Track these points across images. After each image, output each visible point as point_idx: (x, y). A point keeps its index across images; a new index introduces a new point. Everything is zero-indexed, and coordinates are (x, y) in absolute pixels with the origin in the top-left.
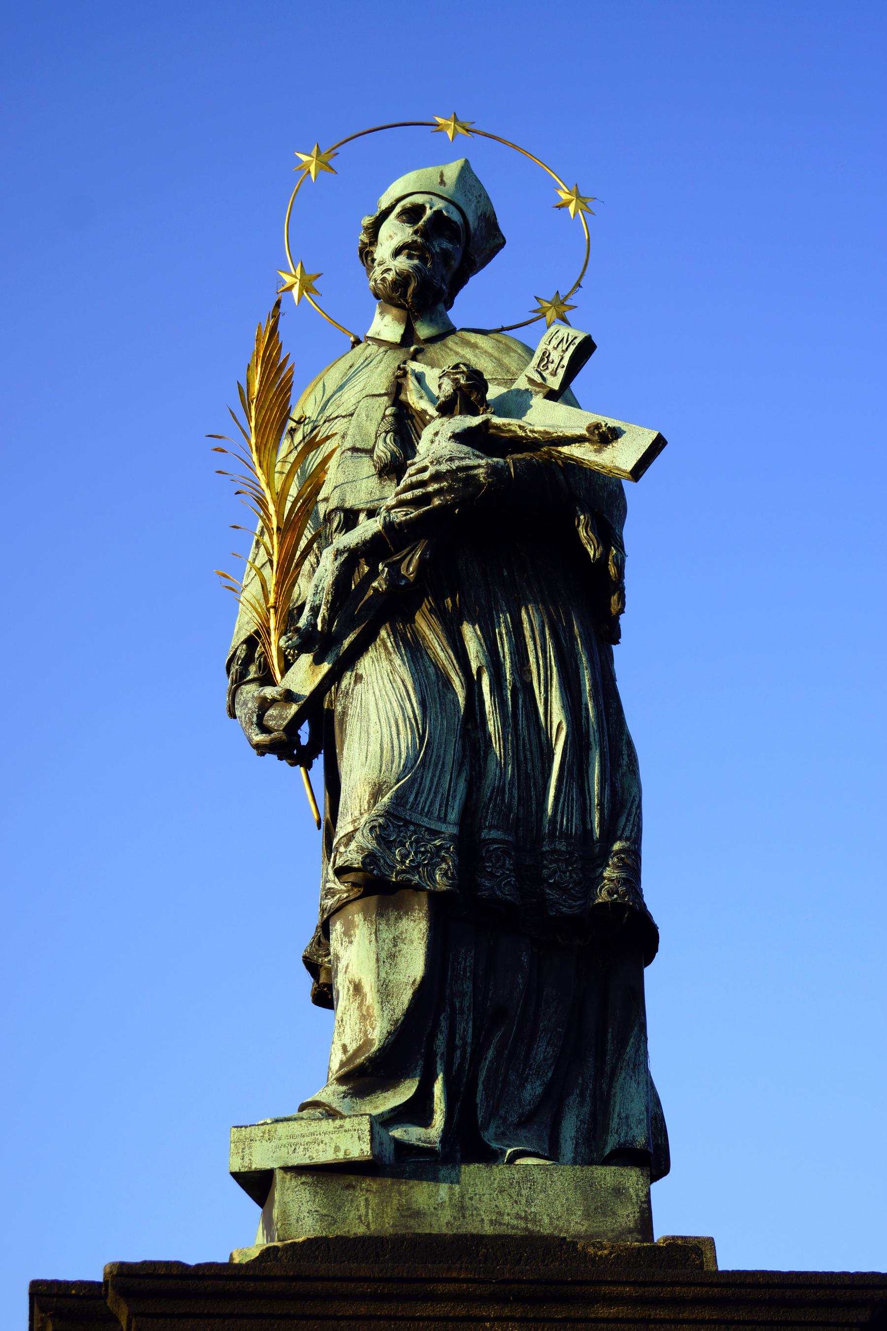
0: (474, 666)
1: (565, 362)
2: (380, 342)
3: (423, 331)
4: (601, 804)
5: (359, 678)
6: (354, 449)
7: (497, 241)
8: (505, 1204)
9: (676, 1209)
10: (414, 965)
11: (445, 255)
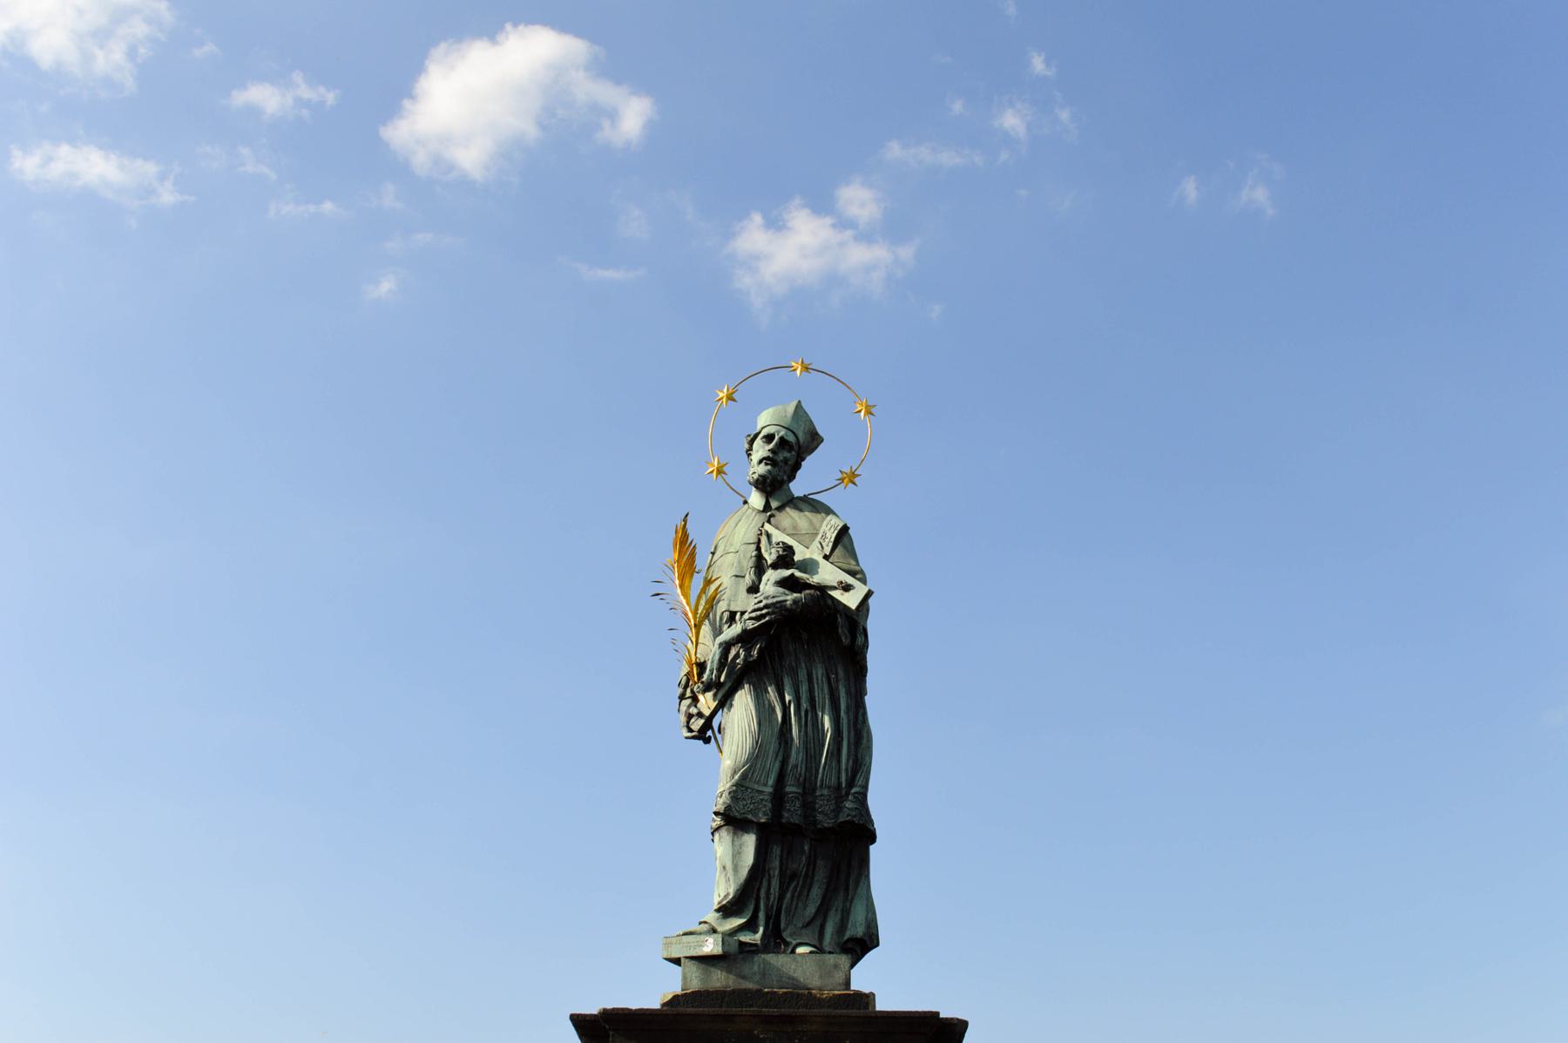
3: (774, 504)
9: (865, 976)
10: (749, 858)
11: (786, 461)
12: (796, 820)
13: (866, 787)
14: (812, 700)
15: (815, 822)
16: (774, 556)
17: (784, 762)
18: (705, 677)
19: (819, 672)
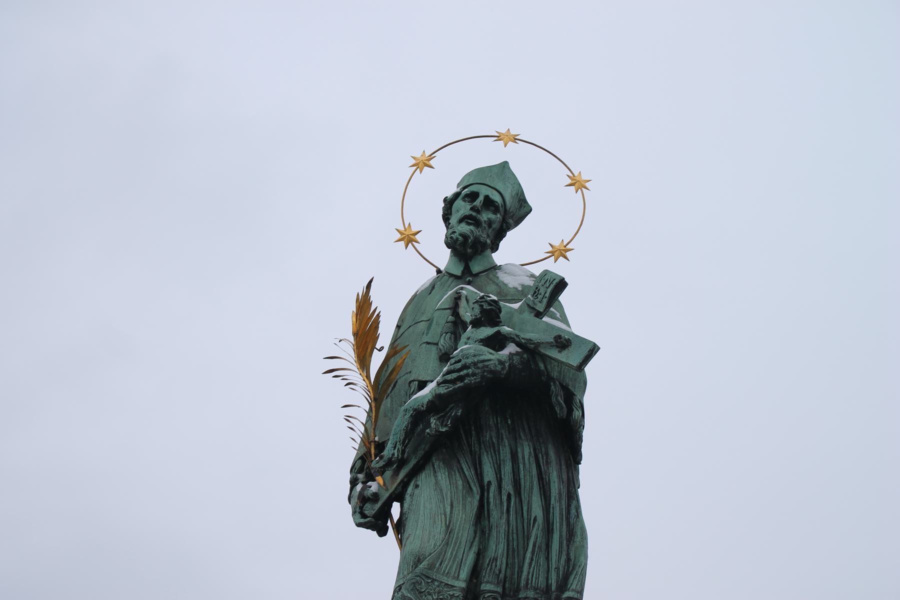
0: (486, 481)
1: (547, 295)
2: (451, 275)
4: (557, 568)
5: (417, 486)
6: (428, 343)
7: (526, 209)
11: (490, 223)
13: (581, 592)
14: (517, 484)
16: (477, 310)
17: (479, 555)
19: (526, 451)
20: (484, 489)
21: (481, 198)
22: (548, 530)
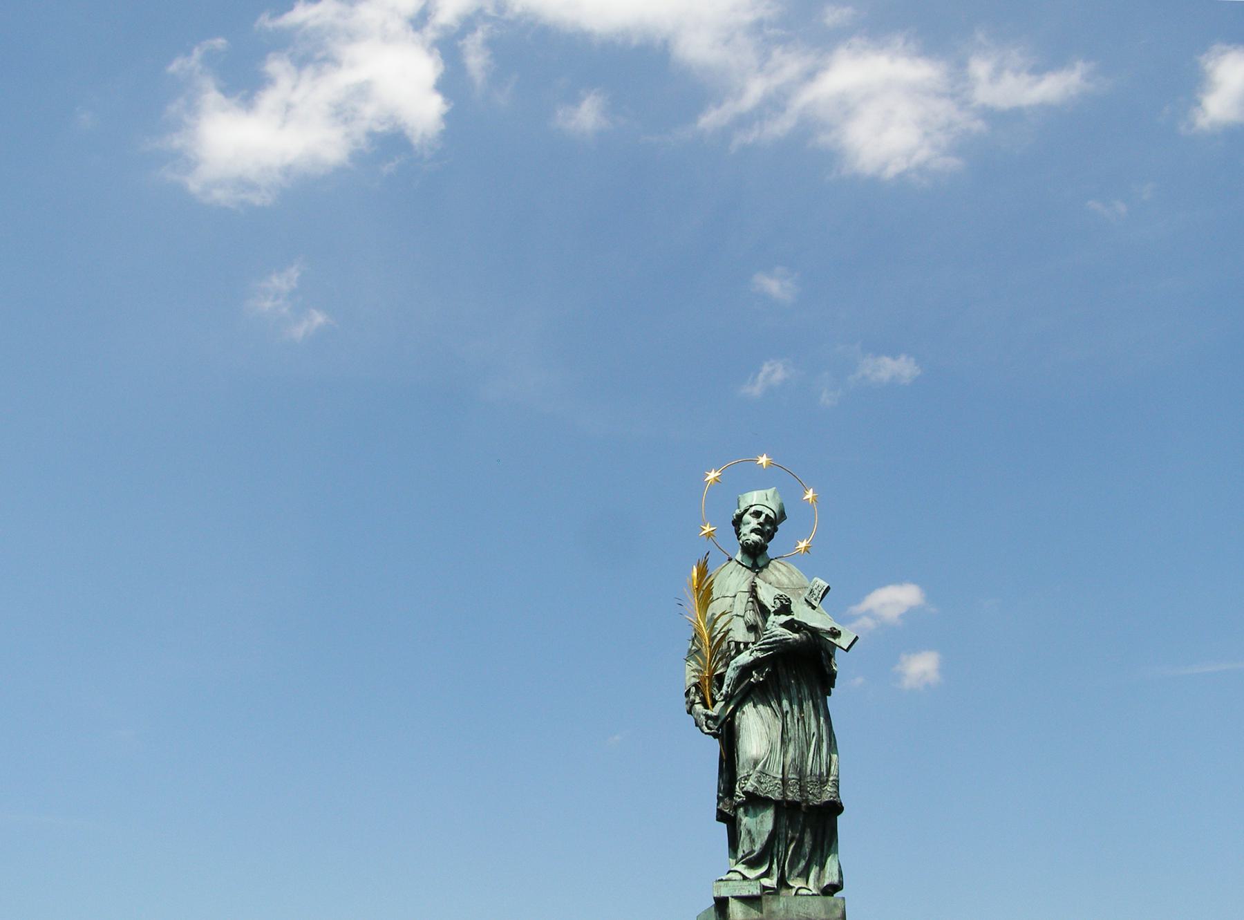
3: (761, 563)
8: (800, 909)
12: (798, 799)
15: (807, 800)
18: (723, 691)
20: (784, 715)
21: (763, 516)
22: (820, 740)
